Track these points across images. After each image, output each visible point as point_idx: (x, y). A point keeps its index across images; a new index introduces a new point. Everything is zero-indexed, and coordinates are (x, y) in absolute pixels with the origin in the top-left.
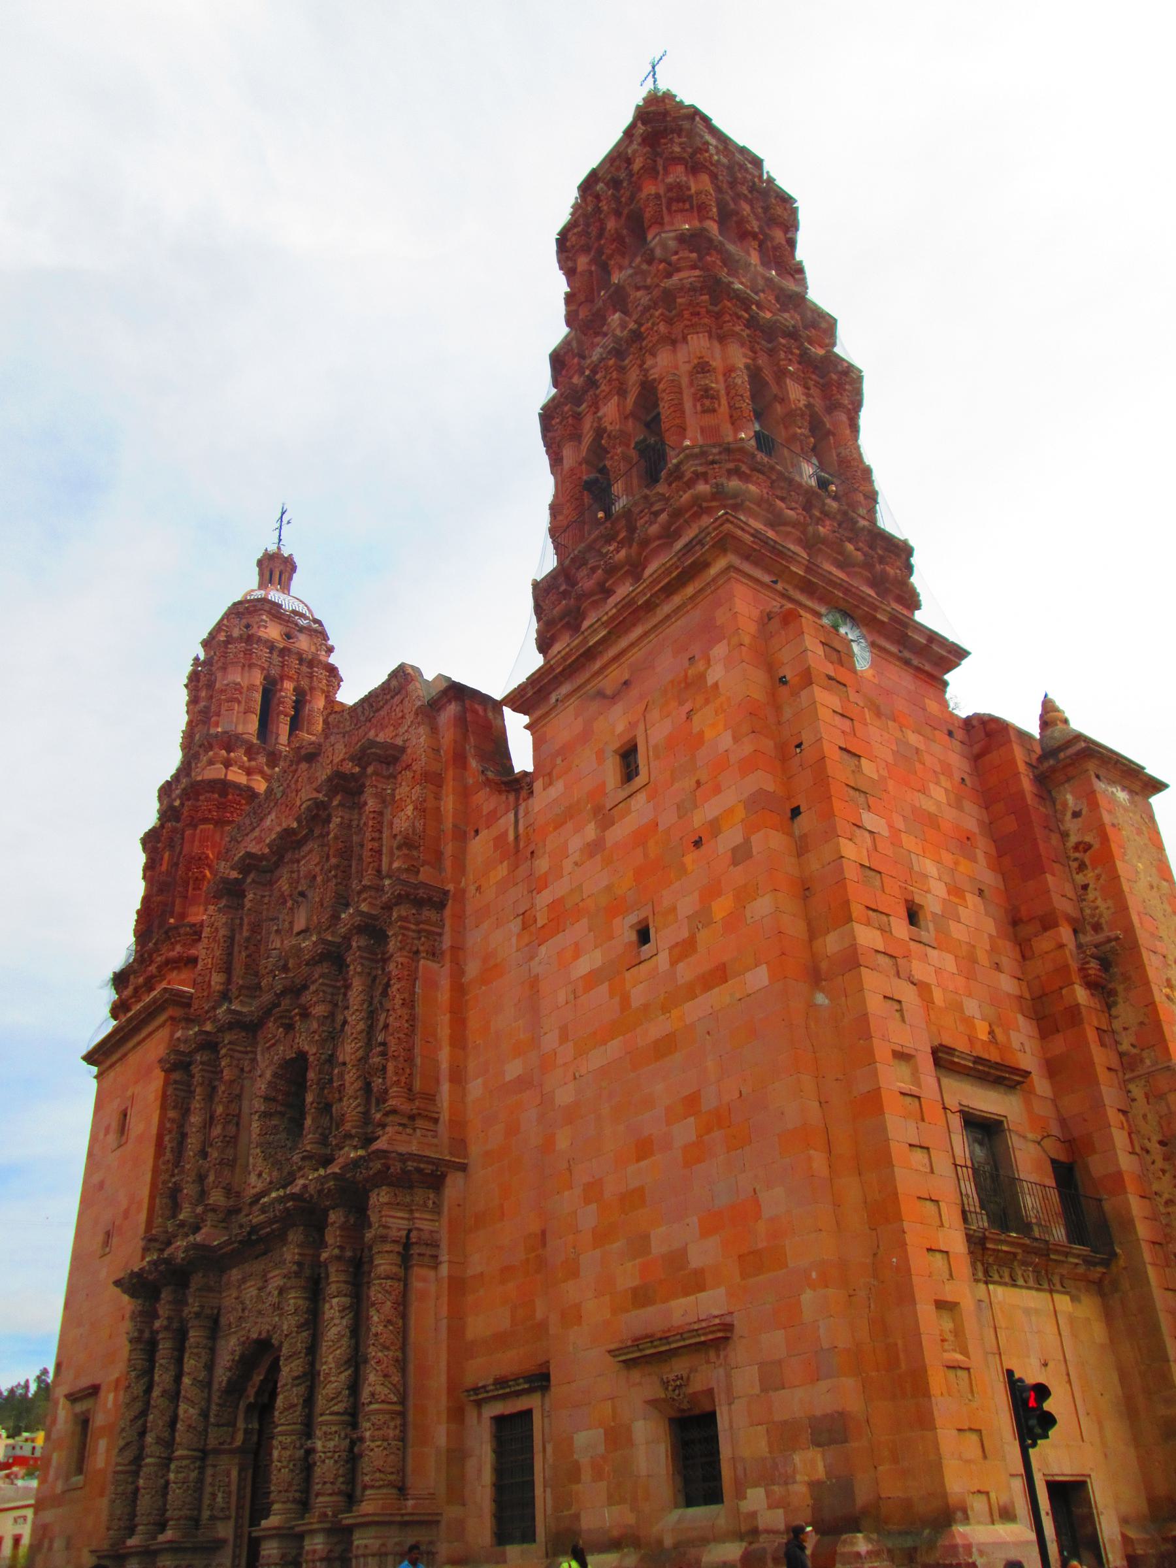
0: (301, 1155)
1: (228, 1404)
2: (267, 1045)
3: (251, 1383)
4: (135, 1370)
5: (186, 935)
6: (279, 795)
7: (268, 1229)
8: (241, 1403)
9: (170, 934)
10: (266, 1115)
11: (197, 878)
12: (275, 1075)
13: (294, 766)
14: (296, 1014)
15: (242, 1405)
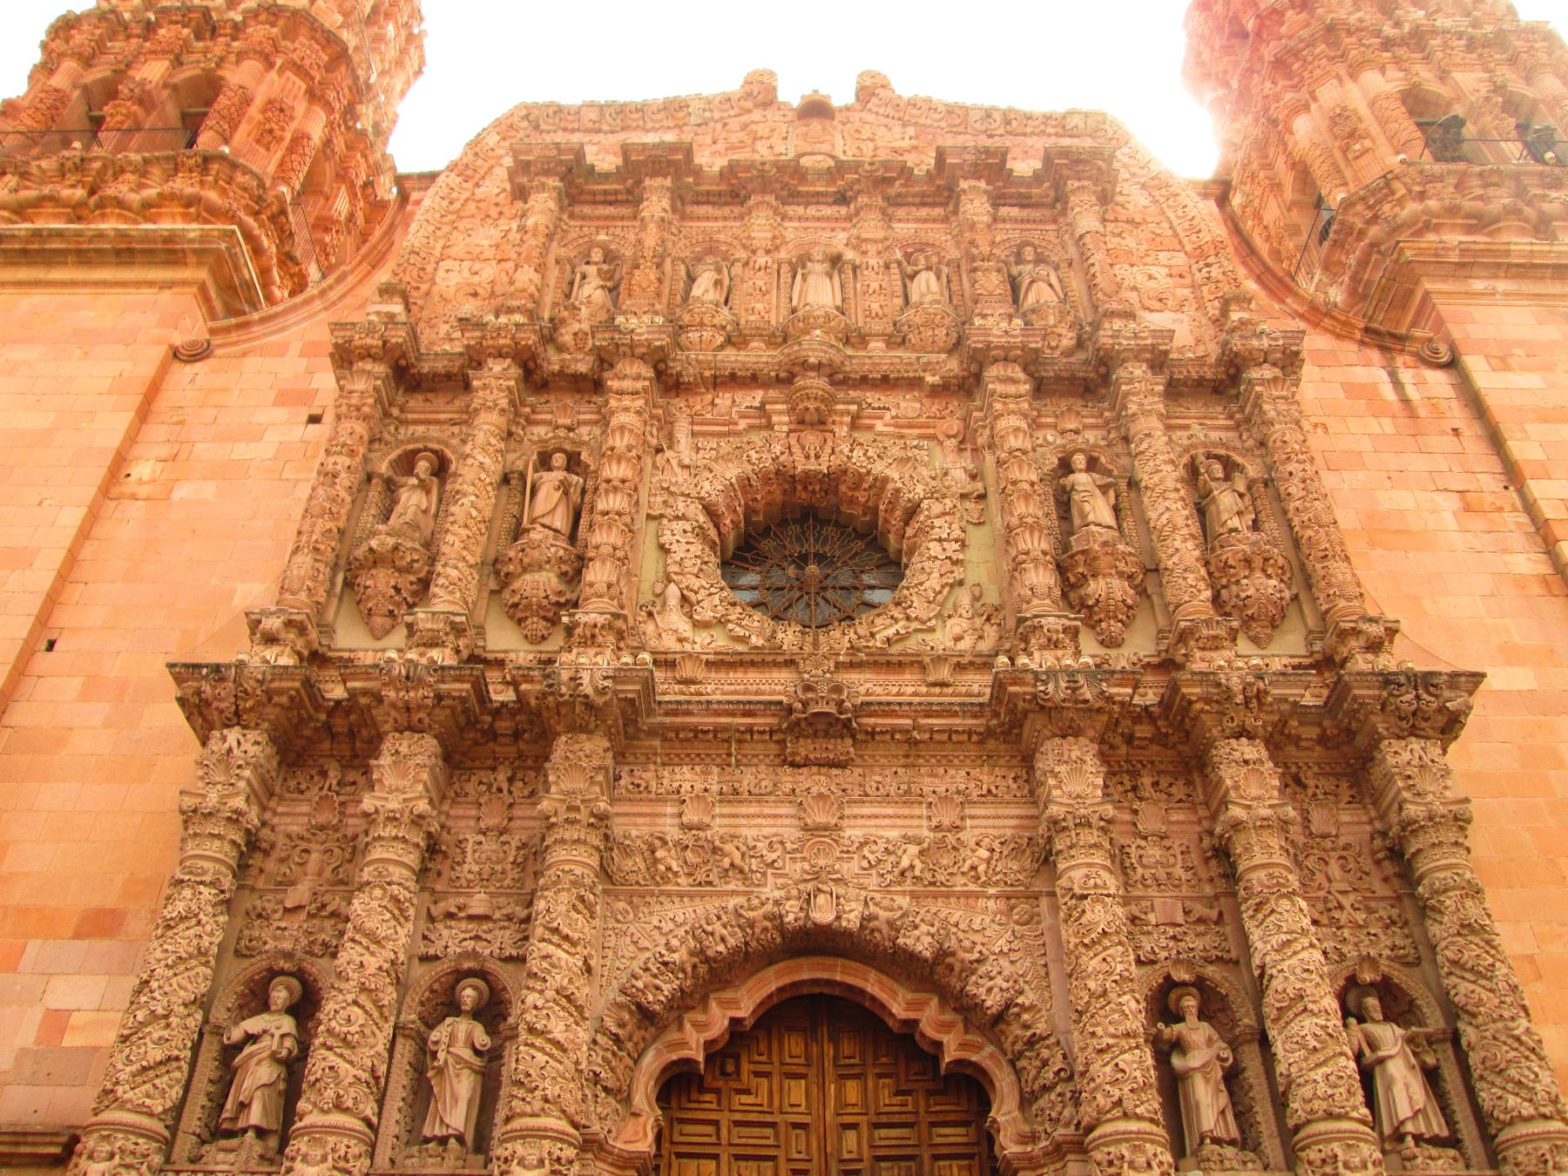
0: (1067, 623)
1: (629, 1045)
2: (696, 428)
3: (701, 1017)
4: (212, 884)
5: (245, 189)
6: (693, 120)
7: (909, 721)
8: (649, 1057)
9: (215, 167)
10: (700, 533)
11: (271, 131)
12: (745, 483)
13: (749, 105)
14: (842, 413)
15: (652, 1062)
